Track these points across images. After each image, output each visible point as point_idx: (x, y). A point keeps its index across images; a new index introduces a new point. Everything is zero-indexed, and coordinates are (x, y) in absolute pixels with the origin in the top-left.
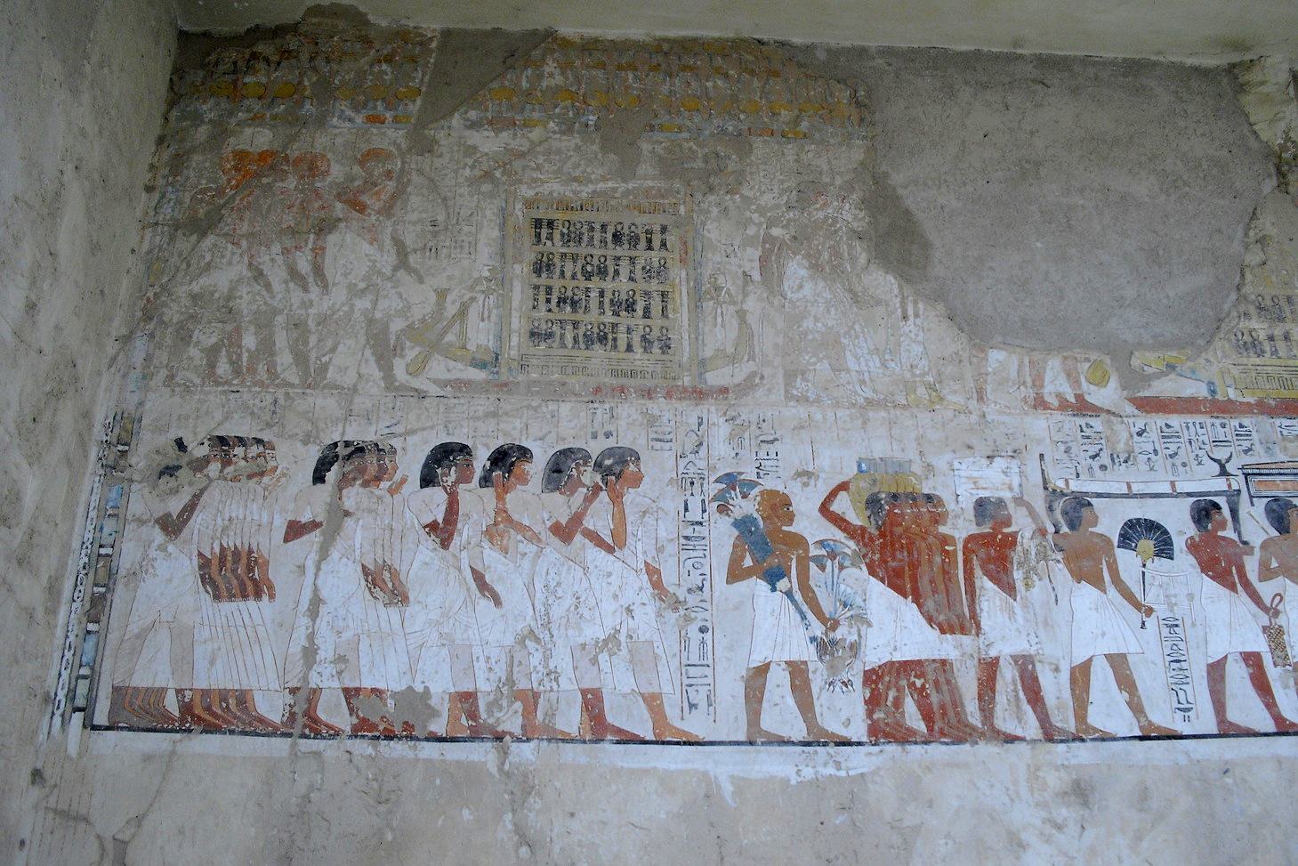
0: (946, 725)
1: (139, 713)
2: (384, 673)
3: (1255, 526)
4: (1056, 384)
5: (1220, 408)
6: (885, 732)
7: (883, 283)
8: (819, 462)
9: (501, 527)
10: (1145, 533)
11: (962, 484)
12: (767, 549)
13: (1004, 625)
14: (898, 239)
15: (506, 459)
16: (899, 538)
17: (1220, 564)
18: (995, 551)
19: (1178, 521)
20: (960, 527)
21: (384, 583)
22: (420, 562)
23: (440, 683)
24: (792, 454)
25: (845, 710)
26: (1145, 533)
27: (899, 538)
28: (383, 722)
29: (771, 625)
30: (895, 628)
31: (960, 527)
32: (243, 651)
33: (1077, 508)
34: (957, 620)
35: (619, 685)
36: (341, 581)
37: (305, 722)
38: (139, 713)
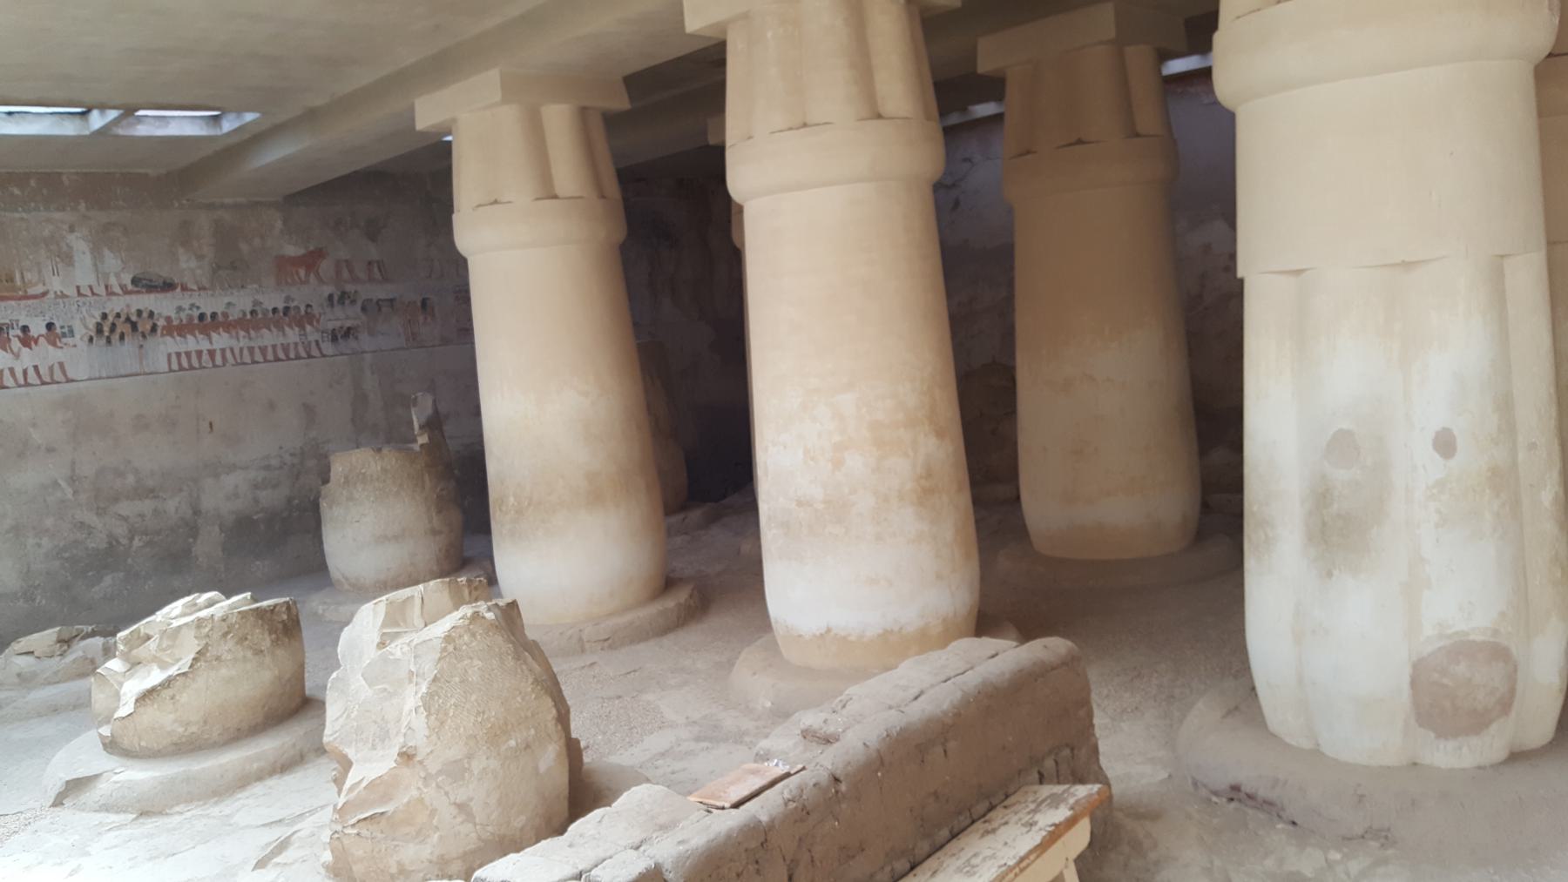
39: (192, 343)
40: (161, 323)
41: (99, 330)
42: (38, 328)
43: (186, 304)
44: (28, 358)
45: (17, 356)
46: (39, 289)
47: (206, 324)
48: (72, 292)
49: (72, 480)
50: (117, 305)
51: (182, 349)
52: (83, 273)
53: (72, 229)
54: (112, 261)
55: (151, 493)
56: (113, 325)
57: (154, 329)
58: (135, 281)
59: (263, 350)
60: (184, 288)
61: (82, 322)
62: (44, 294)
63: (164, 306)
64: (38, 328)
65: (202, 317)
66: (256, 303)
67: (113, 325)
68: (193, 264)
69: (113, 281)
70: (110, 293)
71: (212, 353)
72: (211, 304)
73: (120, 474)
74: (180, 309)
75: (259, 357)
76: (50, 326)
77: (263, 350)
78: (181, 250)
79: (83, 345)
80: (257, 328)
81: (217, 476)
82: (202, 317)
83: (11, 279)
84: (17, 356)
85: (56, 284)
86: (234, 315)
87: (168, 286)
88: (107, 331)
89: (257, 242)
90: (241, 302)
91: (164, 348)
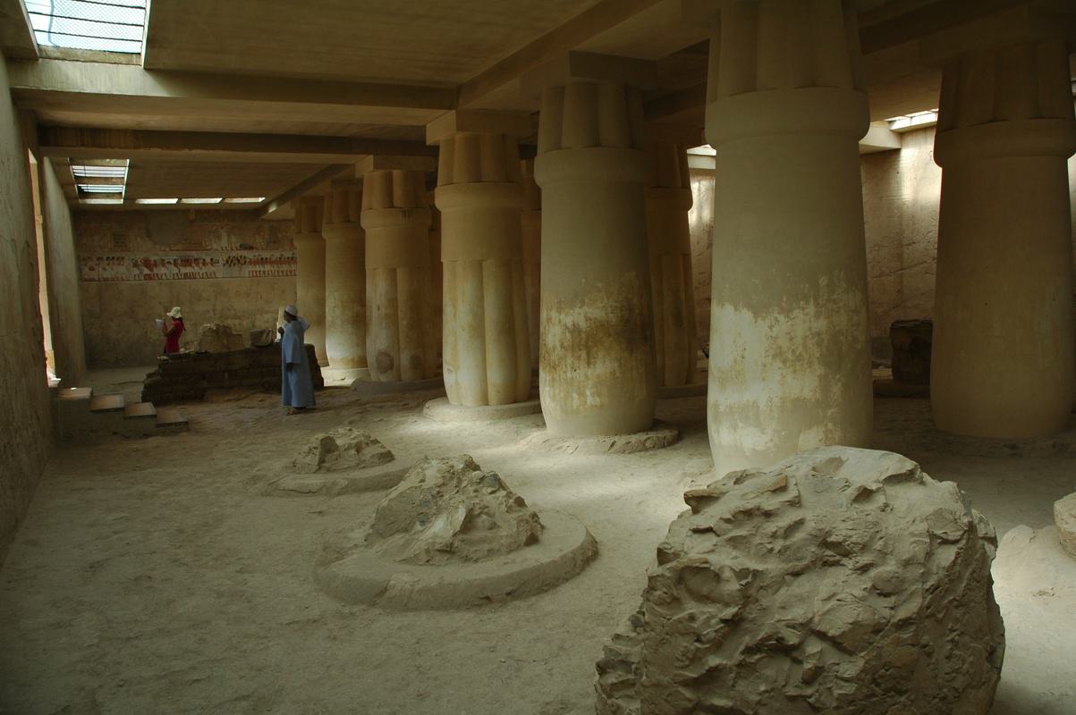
0: (151, 279)
1: (86, 280)
2: (105, 276)
3: (179, 262)
4: (163, 249)
5: (178, 250)
6: (145, 279)
7: (147, 239)
8: (140, 257)
9: (114, 264)
10: (169, 263)
11: (153, 258)
12: (136, 265)
13: (155, 271)
14: (149, 235)
15: (113, 258)
16: (147, 264)
17: (175, 265)
18: (155, 265)
19: (172, 261)
20: (152, 262)
21: (104, 269)
22: (107, 267)
23: (110, 276)
24: (138, 257)
25: (142, 278)
26: (169, 263)
27: (147, 264)
28: (106, 280)
29: (136, 271)
30: (146, 271)
31: (152, 262)
32: (93, 275)
33: (163, 260)
34: (151, 270)
35: (124, 276)
36: (100, 269)
37: (99, 280)
38: (86, 280)
39: (258, 268)
40: (248, 260)
41: (227, 262)
42: (208, 260)
43: (257, 254)
44: (204, 270)
45: (201, 269)
46: (209, 248)
47: (263, 261)
48: (220, 249)
49: (214, 310)
50: (234, 254)
51: (254, 269)
52: (224, 243)
53: (222, 228)
54: (233, 239)
55: (239, 318)
56: (232, 261)
57: (245, 262)
58: (240, 246)
59: (282, 272)
60: (257, 249)
61: (222, 259)
62: (211, 249)
63: (249, 255)
64: (208, 260)
65: (262, 259)
66: (282, 255)
67: (232, 261)
68: (261, 240)
69: (233, 246)
70: (232, 250)
71: (264, 272)
72: (266, 255)
73: (229, 310)
74: (255, 256)
75: (281, 274)
76: (212, 260)
77: (282, 272)
78: (257, 236)
79: (222, 267)
80: (281, 264)
81: (261, 314)
82: (262, 259)
83: (201, 243)
84: (201, 269)
85: (215, 246)
86: (274, 259)
87: (251, 248)
88: (230, 262)
89: (284, 233)
90: (277, 254)
91: (248, 269)
